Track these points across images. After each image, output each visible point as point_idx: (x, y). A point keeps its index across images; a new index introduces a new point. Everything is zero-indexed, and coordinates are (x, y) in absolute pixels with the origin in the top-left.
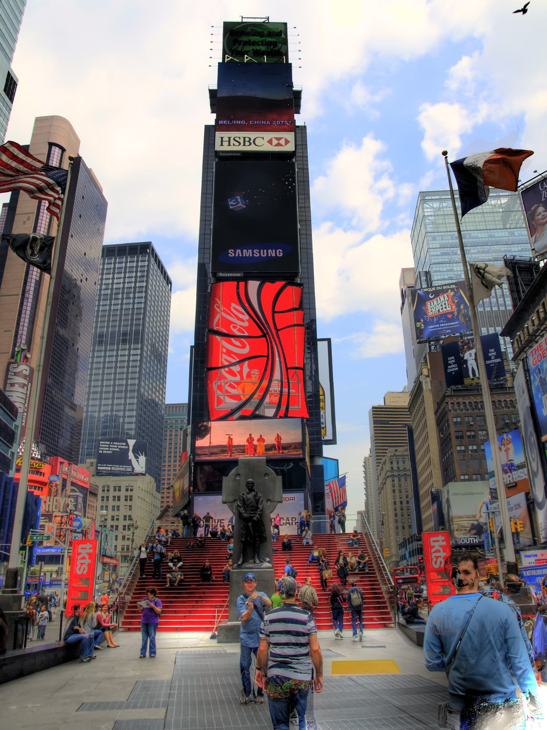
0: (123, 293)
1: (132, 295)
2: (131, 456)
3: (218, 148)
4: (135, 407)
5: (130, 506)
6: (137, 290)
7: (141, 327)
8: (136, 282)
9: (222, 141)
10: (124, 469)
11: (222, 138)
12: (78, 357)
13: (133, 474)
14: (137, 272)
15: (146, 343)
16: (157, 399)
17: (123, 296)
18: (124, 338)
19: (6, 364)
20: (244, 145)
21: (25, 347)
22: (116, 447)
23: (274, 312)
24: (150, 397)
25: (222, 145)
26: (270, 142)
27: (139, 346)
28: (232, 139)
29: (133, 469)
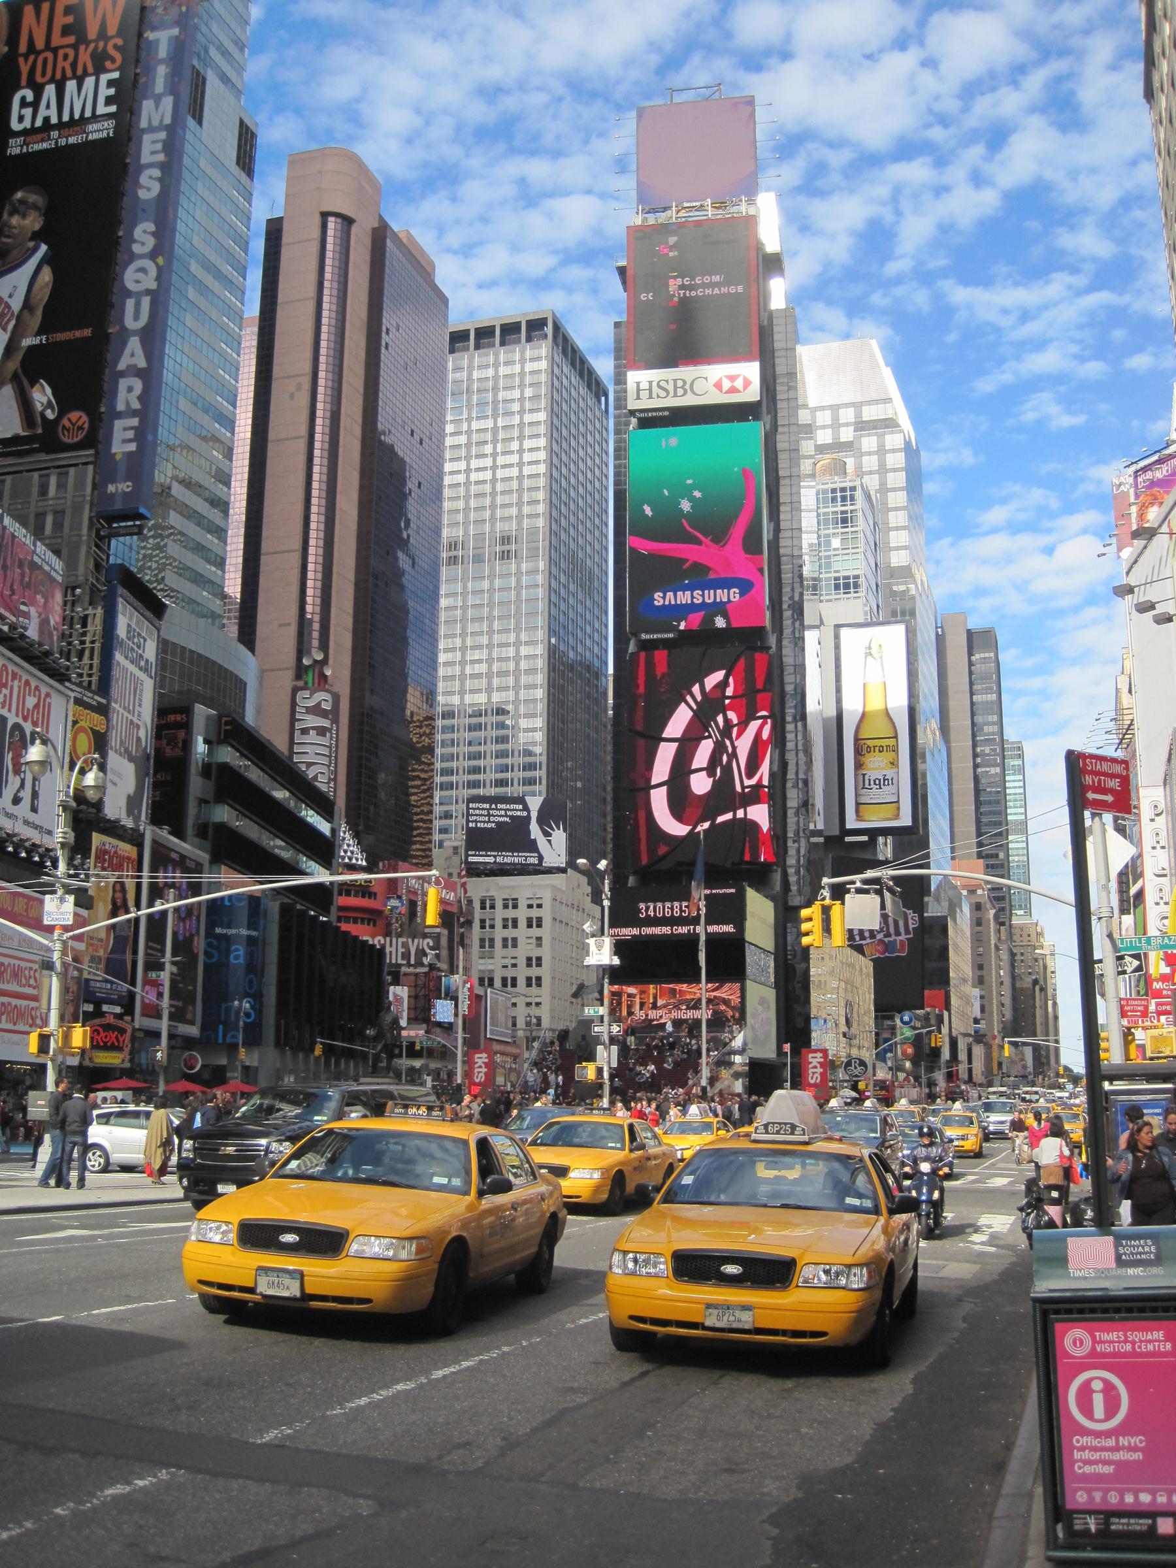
0: (495, 442)
1: (515, 446)
2: (535, 831)
5: (539, 939)
10: (522, 860)
12: (402, 587)
13: (539, 870)
14: (522, 386)
17: (495, 448)
19: (289, 691)
20: (675, 395)
21: (319, 657)
22: (502, 814)
25: (638, 398)
26: (718, 385)
29: (541, 858)
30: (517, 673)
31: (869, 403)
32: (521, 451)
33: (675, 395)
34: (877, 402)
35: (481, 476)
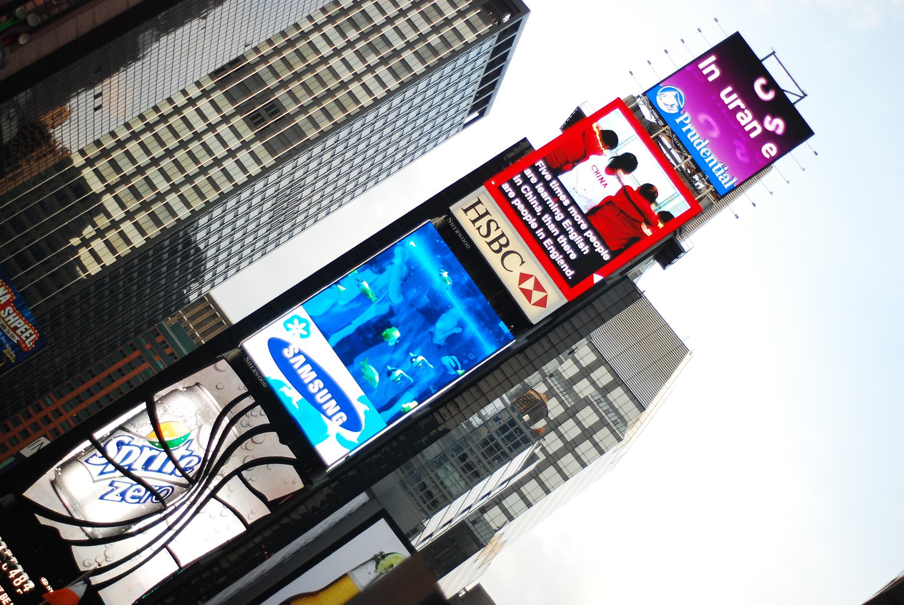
0: (364, 36)
1: (372, 59)
3: (457, 209)
4: (124, 250)
6: (394, 62)
7: (312, 134)
8: (410, 45)
9: (473, 206)
11: (479, 202)
14: (435, 29)
15: (288, 168)
16: (210, 265)
17: (357, 41)
18: (264, 114)
20: (490, 244)
21: (32, 21)
23: (238, 472)
24: (202, 246)
25: (466, 211)
26: (524, 277)
27: (269, 161)
28: (487, 218)
30: (145, 206)
31: (628, 391)
32: (370, 69)
33: (490, 244)
34: (633, 398)
35: (321, 44)
